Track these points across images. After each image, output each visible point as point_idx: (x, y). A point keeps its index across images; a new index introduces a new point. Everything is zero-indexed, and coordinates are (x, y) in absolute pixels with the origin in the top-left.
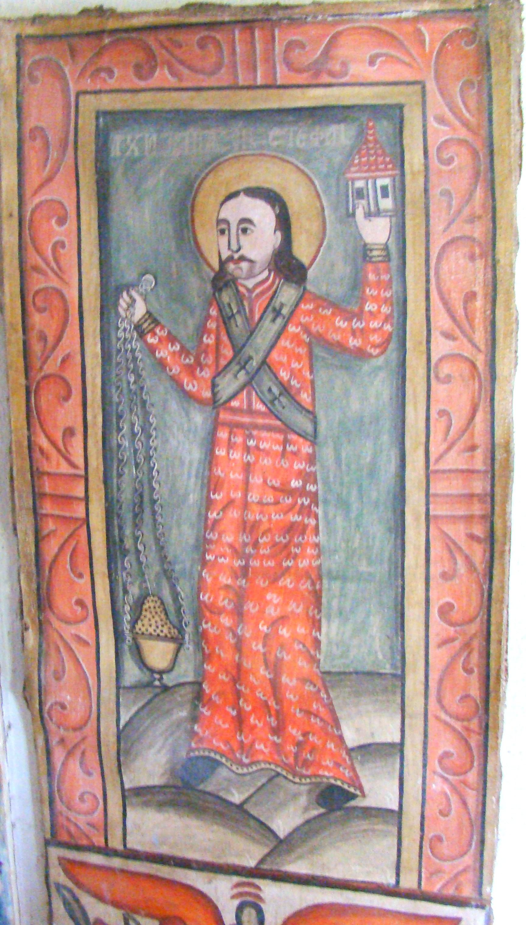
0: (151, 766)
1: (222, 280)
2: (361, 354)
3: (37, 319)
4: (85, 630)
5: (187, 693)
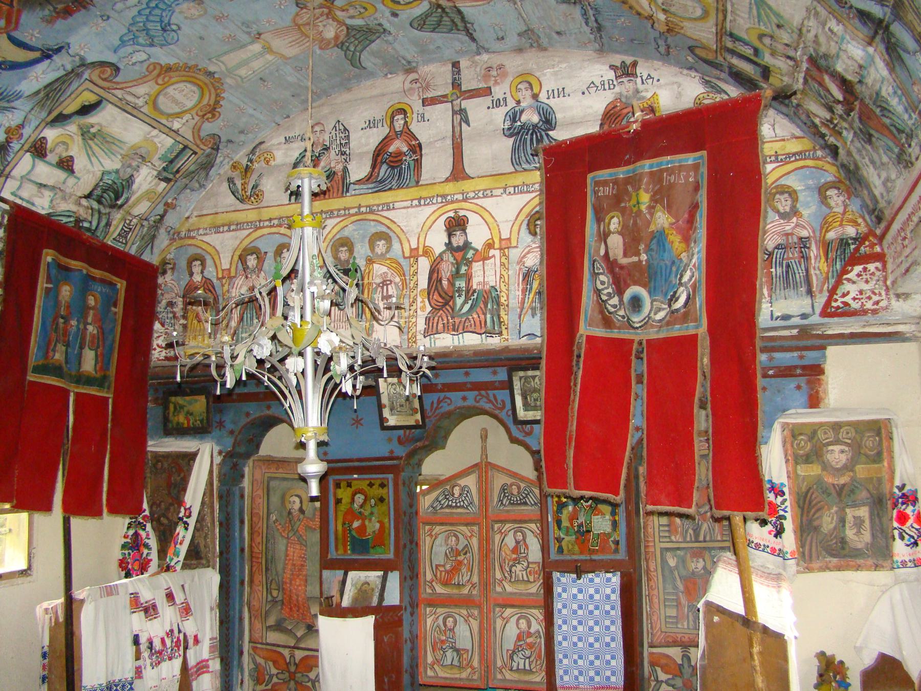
0: (271, 621)
1: (290, 513)
2: (315, 529)
3: (254, 519)
4: (260, 588)
5: (280, 603)
